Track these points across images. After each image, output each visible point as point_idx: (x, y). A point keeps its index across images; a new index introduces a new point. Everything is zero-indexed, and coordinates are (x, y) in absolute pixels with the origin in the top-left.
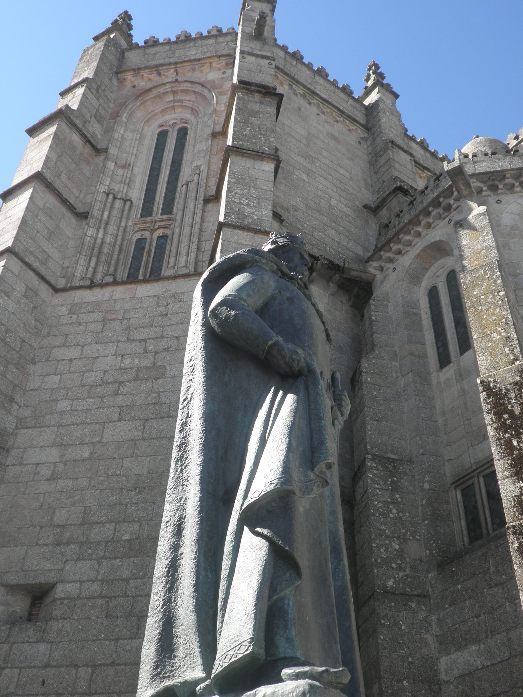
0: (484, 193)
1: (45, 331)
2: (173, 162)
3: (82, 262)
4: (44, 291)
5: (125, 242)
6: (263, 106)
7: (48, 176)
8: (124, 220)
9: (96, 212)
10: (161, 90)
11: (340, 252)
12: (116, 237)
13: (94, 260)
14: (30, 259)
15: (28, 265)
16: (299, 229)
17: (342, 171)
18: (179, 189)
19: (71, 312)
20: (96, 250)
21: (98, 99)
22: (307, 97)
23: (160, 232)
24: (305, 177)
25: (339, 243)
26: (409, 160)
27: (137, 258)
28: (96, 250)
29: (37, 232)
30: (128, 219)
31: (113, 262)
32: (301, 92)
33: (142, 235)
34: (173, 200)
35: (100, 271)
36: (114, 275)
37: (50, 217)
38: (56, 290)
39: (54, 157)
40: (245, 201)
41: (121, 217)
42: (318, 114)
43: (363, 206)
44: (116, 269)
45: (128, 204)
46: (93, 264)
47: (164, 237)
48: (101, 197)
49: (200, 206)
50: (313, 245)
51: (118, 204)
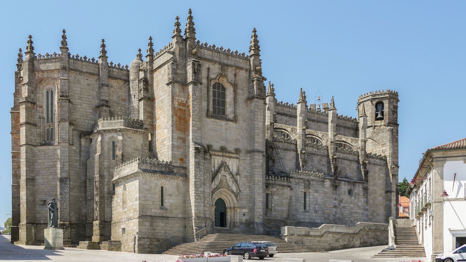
1: (35, 156)
4: (33, 148)
14: (29, 143)
15: (29, 145)
19: (39, 152)
23: (51, 127)
24: (80, 107)
27: (48, 134)
34: (53, 117)
36: (44, 141)
38: (35, 146)
40: (63, 134)
46: (40, 139)
47: (52, 129)
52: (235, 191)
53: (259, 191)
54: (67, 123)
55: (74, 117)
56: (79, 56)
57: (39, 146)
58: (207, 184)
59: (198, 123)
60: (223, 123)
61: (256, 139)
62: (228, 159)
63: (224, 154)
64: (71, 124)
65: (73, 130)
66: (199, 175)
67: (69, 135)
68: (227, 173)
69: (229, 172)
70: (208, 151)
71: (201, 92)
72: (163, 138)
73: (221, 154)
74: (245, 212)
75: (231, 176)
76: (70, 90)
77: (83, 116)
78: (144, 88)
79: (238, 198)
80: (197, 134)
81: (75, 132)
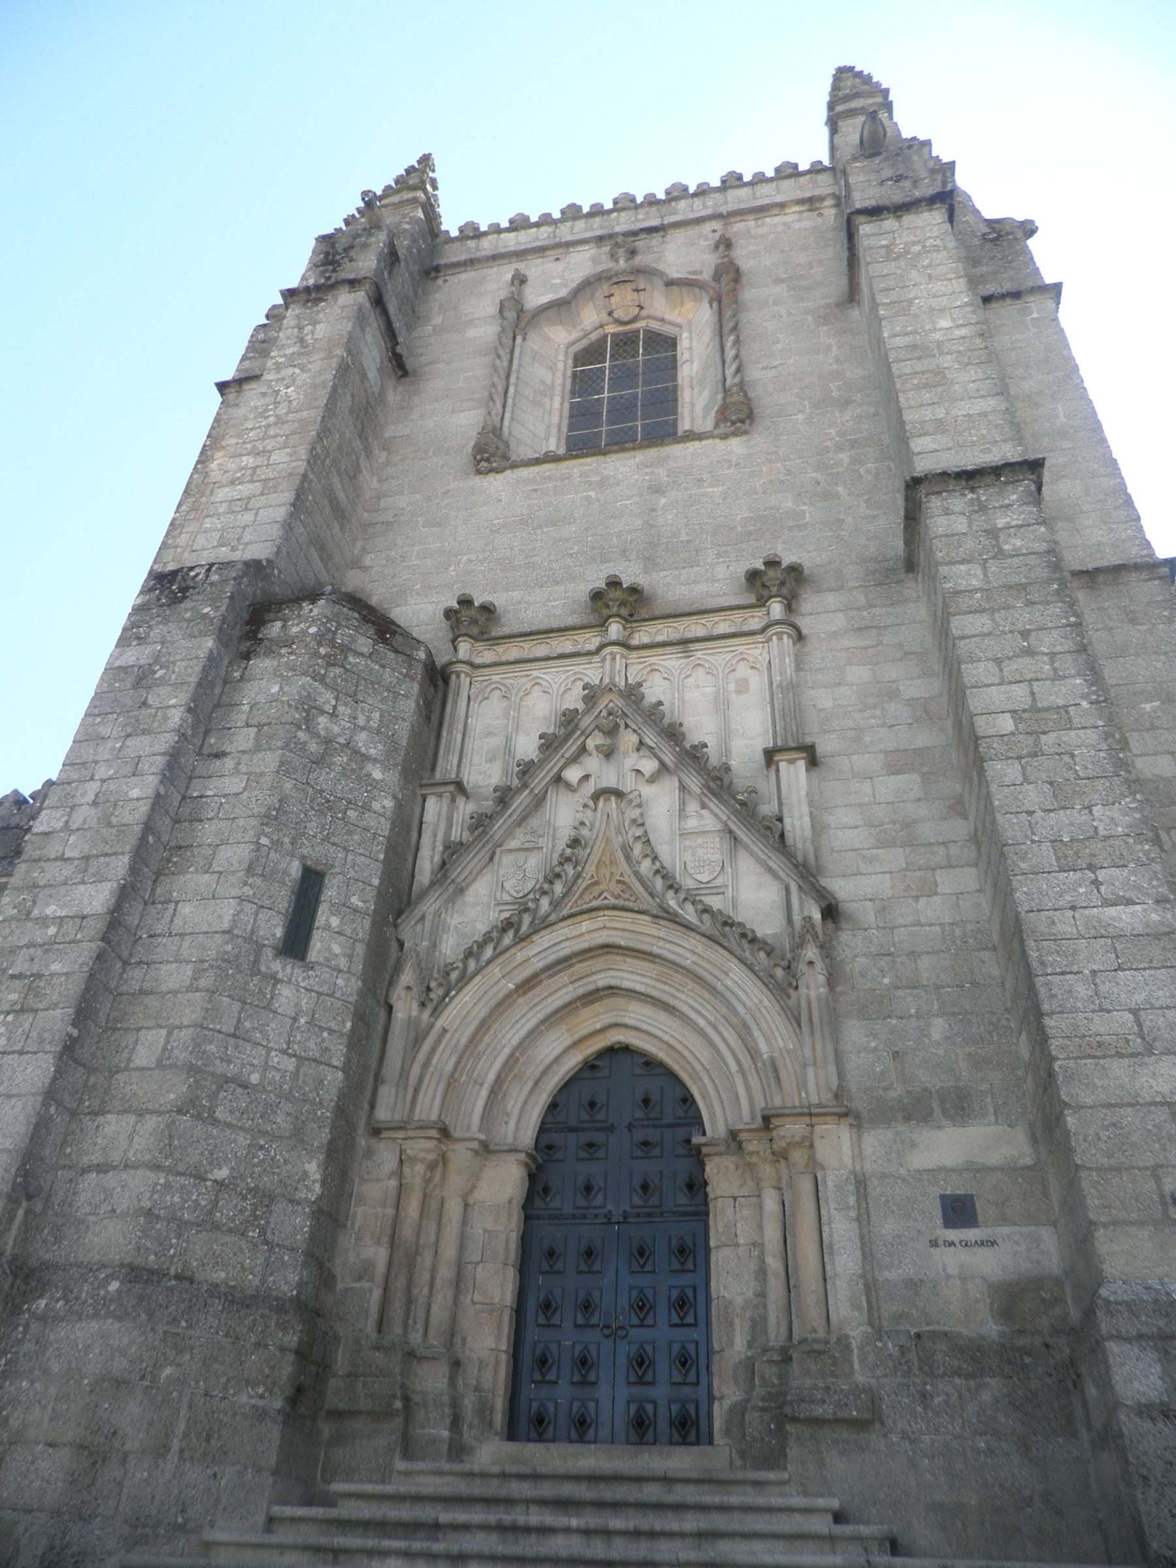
52: (768, 926)
53: (1067, 823)
58: (224, 853)
61: (908, 416)
62: (671, 661)
63: (615, 629)
66: (102, 772)
68: (649, 766)
69: (669, 759)
73: (591, 641)
74: (976, 1170)
75: (694, 783)
79: (814, 984)
80: (248, 518)
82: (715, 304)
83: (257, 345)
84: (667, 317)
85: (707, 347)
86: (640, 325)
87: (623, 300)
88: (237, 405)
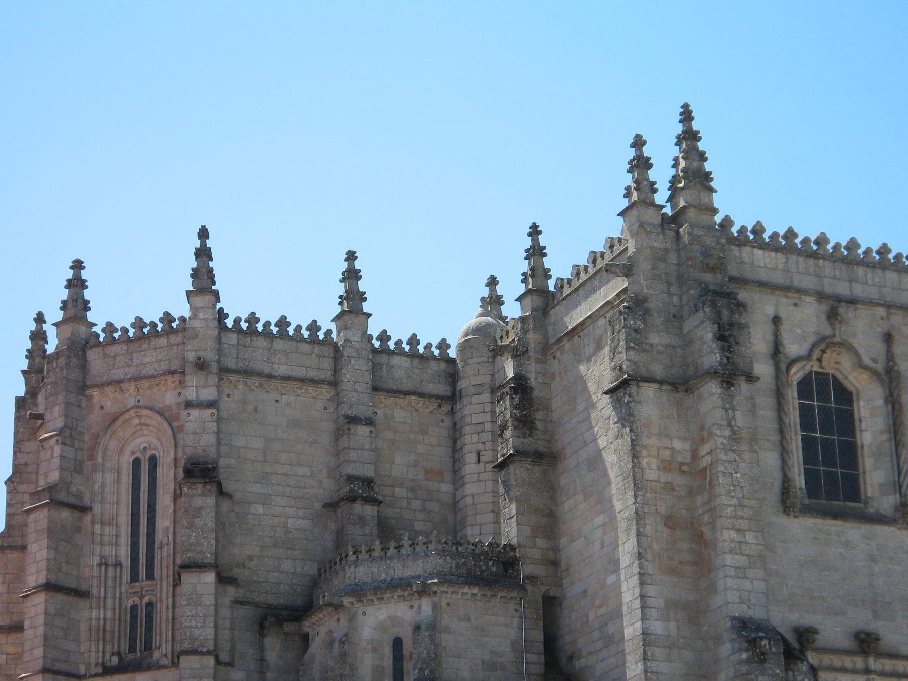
0: (356, 606)
2: (149, 506)
3: (93, 649)
5: (122, 611)
6: (204, 499)
7: (53, 579)
8: (117, 589)
9: (95, 591)
10: (126, 416)
11: (293, 584)
12: (114, 609)
13: (101, 642)
16: (255, 581)
17: (301, 471)
18: (156, 551)
20: (101, 631)
21: (72, 446)
22: (264, 386)
23: (146, 600)
25: (293, 573)
26: (368, 433)
27: (133, 628)
28: (101, 631)
29: (56, 638)
30: (120, 587)
31: (116, 639)
32: (257, 385)
33: (134, 601)
34: (153, 558)
35: (108, 650)
36: (118, 654)
37: (63, 616)
39: (53, 552)
41: (115, 588)
42: (277, 401)
43: (323, 507)
44: (119, 647)
45: (118, 569)
46: (101, 649)
47: (150, 605)
48: (96, 572)
49: (171, 588)
50: (267, 593)
51: (111, 569)
54: (210, 577)
55: (236, 551)
56: (258, 320)
57: (96, 675)
59: (749, 537)
60: (853, 531)
64: (224, 579)
65: (237, 602)
67: (216, 626)
70: (802, 650)
71: (753, 411)
72: (603, 611)
76: (224, 449)
77: (275, 546)
78: (515, 418)
81: (244, 612)
82: (890, 407)
83: (633, 334)
84: (850, 378)
85: (882, 433)
86: (832, 372)
87: (830, 358)
88: (639, 402)
